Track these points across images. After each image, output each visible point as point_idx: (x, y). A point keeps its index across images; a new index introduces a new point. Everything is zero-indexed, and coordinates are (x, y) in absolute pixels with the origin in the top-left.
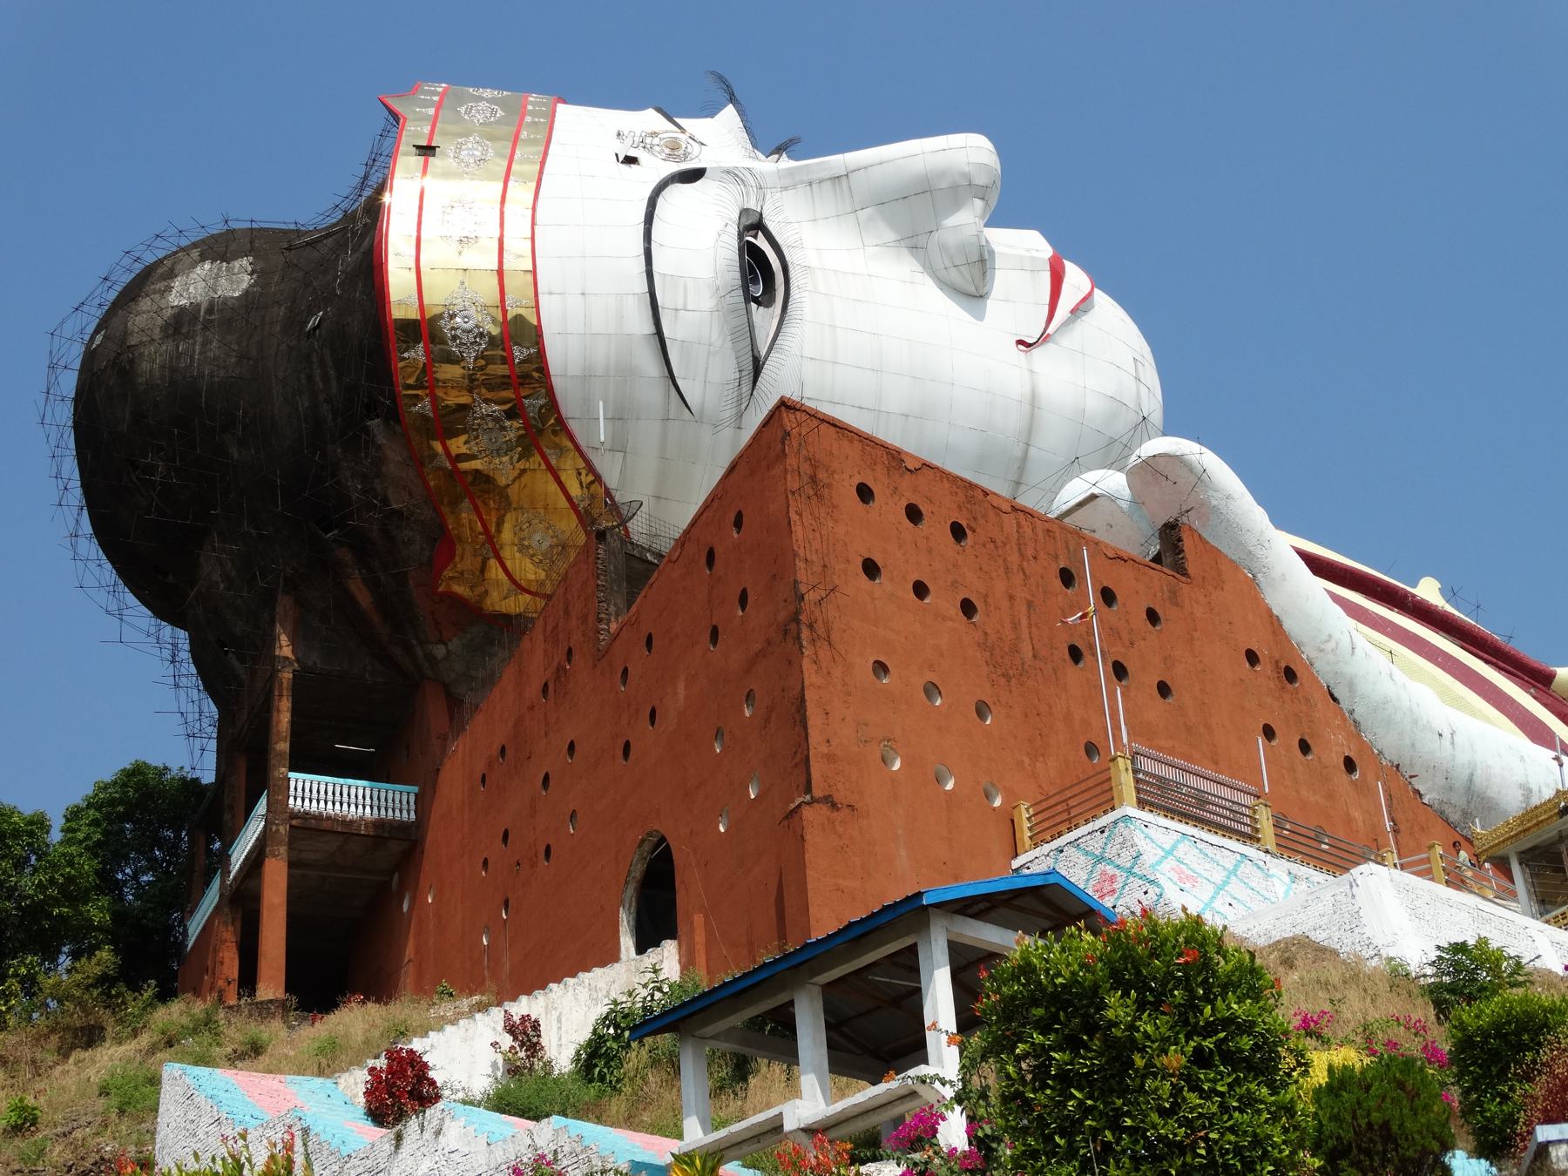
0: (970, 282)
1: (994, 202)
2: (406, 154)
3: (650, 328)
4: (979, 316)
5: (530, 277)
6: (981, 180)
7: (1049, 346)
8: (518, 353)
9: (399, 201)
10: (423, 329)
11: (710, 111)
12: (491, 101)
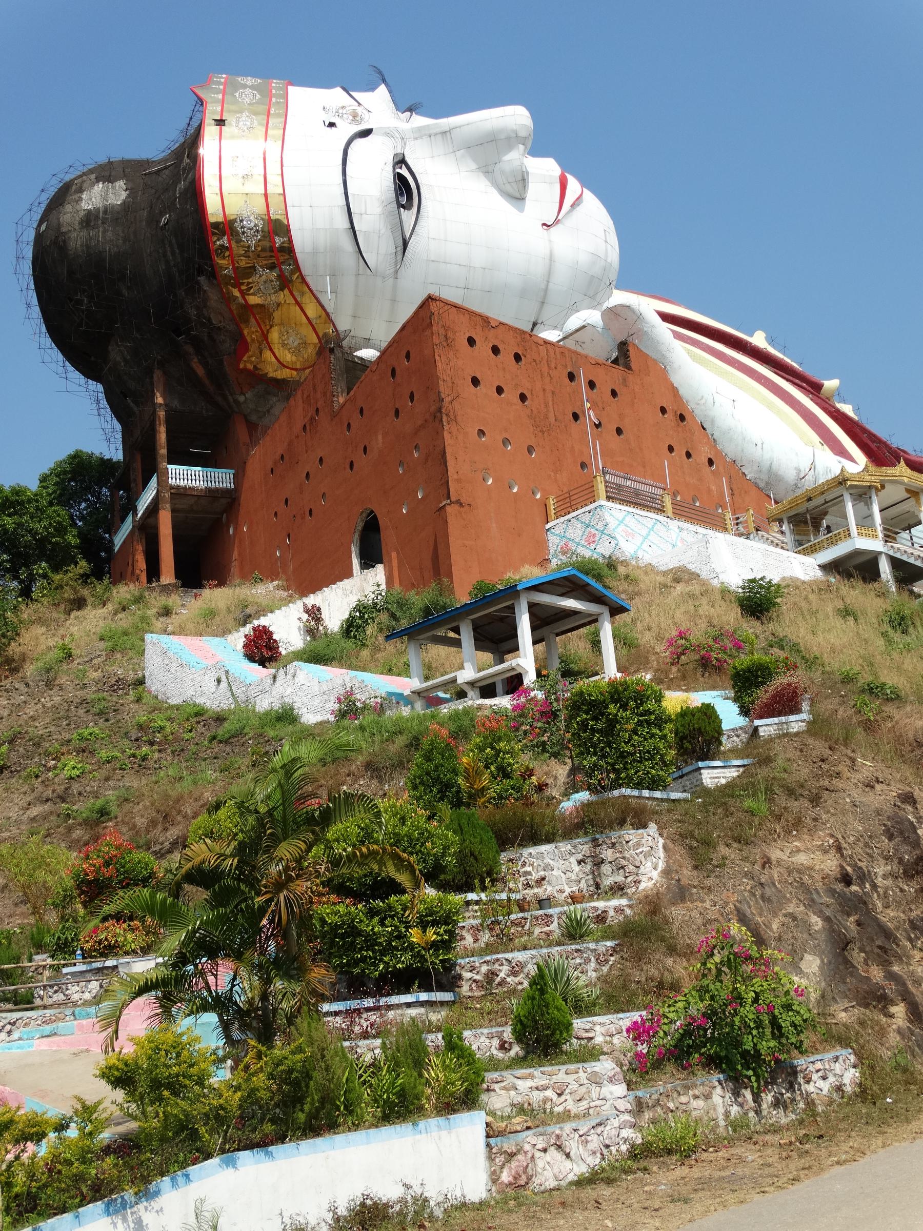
0: (516, 190)
1: (529, 147)
2: (209, 125)
3: (345, 224)
4: (521, 210)
5: (282, 198)
6: (523, 134)
7: (559, 226)
8: (278, 241)
9: (208, 150)
10: (227, 227)
11: (372, 88)
12: (253, 87)
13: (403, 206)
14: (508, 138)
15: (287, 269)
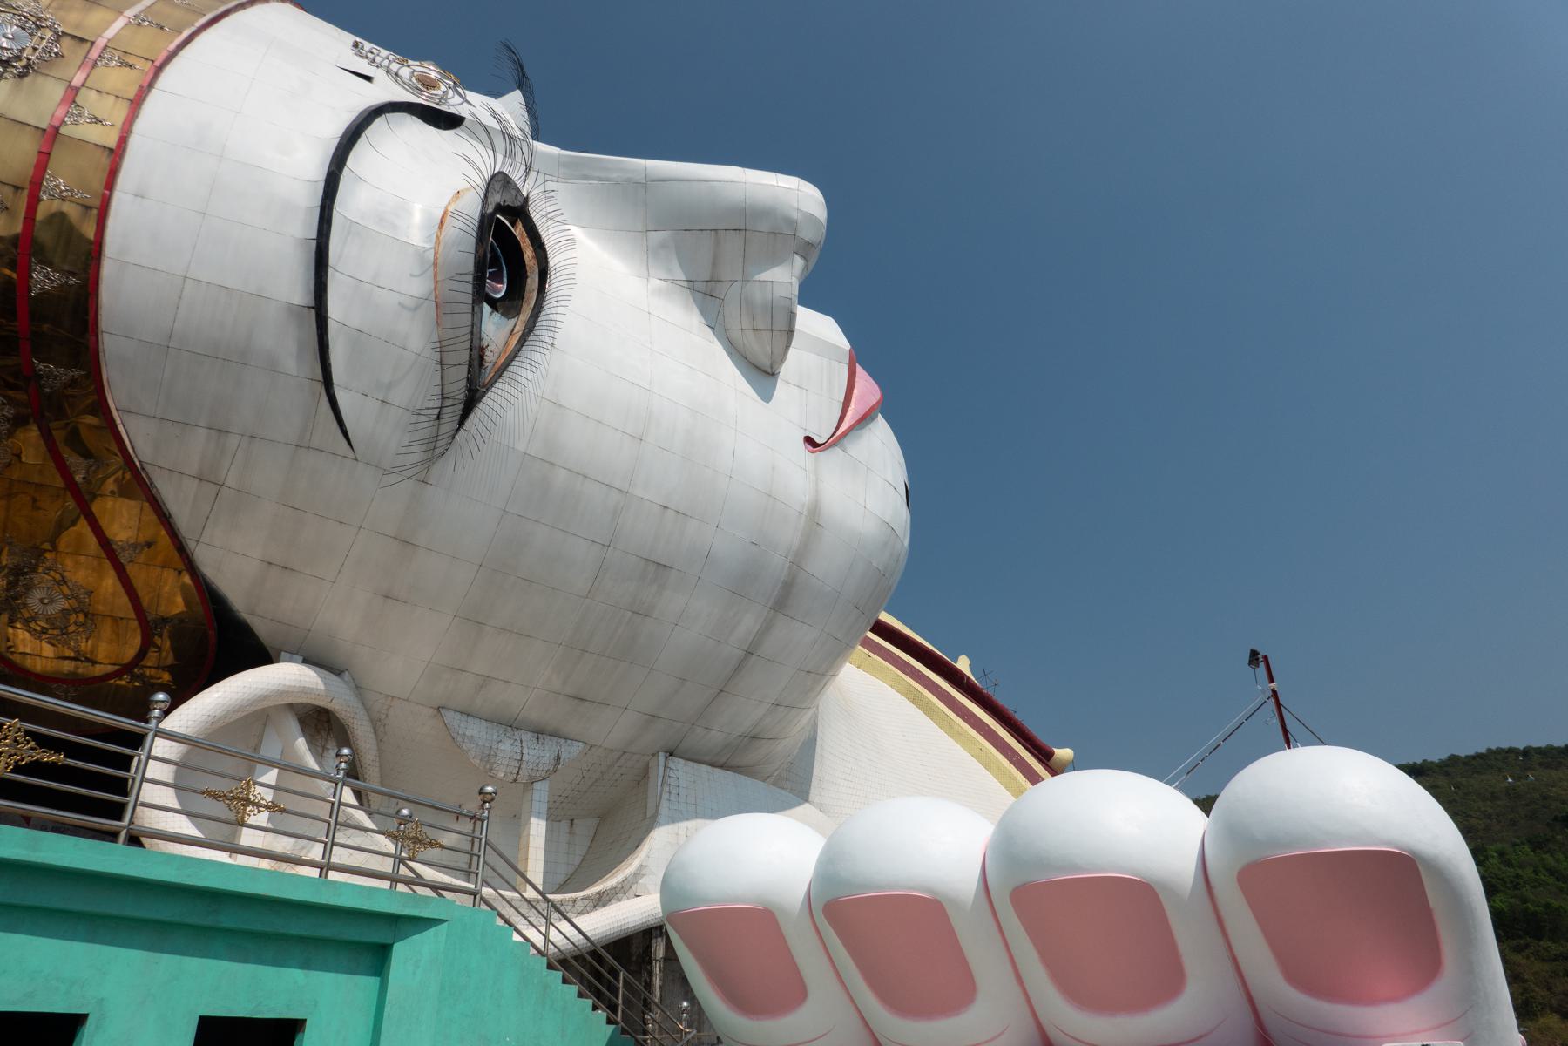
3: (297, 292)
4: (766, 396)
5: (105, 161)
6: (808, 234)
7: (837, 450)
13: (494, 304)
14: (775, 234)
15: (54, 373)
